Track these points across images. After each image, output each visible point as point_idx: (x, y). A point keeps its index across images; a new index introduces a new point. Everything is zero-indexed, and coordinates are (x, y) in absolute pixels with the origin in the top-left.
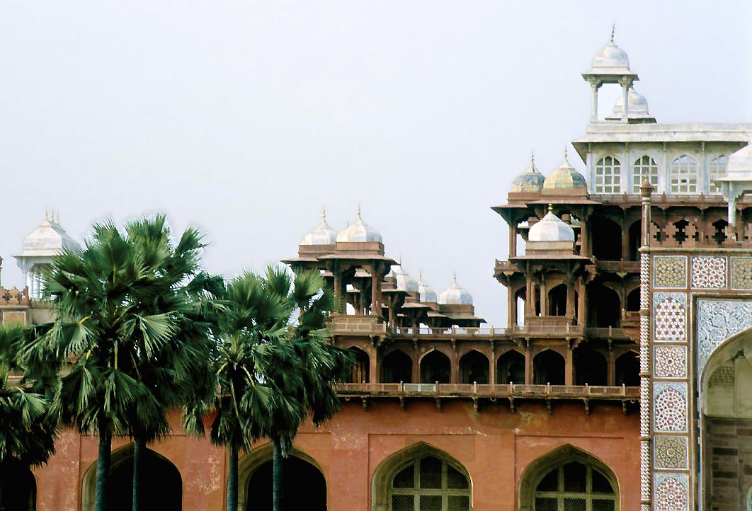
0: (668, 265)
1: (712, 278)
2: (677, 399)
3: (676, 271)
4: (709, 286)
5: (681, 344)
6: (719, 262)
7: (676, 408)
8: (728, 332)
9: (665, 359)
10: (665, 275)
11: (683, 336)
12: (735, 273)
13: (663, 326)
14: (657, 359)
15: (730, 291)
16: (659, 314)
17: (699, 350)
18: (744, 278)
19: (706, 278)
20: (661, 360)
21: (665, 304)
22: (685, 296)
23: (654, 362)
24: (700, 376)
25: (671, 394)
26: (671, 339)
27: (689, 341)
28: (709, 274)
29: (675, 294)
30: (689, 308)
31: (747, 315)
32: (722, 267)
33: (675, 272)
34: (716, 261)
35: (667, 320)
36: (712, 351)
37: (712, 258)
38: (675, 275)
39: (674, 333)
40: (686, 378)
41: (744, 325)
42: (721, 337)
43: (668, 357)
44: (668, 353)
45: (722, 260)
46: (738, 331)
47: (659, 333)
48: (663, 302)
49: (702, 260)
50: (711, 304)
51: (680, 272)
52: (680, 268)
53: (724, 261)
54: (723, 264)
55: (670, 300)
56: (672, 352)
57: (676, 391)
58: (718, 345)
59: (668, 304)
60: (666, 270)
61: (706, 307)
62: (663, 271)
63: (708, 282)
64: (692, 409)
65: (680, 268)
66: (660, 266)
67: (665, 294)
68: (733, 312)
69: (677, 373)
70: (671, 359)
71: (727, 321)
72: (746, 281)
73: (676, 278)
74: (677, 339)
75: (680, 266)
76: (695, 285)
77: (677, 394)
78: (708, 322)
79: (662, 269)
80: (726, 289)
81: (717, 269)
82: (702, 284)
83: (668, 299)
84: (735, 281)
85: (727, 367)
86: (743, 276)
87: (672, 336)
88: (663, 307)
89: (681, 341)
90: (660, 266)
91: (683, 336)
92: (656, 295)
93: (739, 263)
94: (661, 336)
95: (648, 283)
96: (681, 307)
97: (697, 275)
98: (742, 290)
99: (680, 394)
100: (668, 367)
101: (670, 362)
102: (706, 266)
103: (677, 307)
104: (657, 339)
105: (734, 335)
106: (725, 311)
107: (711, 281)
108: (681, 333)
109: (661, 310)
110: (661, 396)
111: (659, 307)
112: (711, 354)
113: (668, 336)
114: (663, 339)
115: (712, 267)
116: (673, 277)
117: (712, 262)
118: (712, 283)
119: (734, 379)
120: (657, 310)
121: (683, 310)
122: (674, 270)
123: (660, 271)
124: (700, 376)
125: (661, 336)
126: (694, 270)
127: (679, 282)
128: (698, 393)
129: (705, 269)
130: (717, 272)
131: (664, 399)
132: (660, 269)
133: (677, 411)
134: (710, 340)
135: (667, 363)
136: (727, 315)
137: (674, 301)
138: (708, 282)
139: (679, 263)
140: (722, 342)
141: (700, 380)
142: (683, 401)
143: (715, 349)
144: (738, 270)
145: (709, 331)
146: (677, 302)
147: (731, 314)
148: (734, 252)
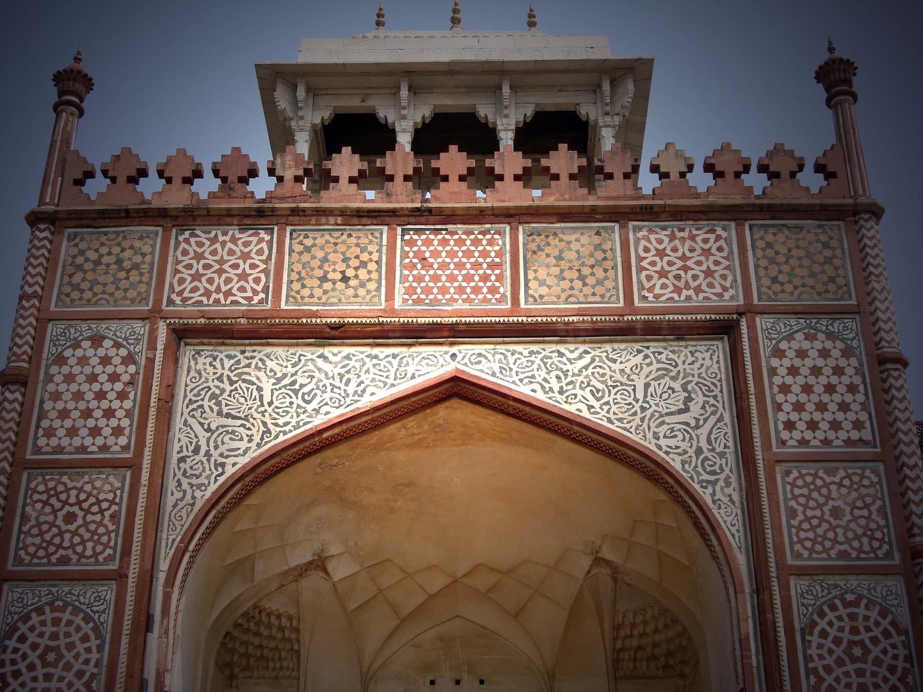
0: (104, 250)
1: (228, 281)
2: (76, 638)
3: (127, 264)
4: (217, 301)
5: (115, 465)
6: (254, 239)
7: (68, 667)
8: (269, 431)
9: (54, 512)
10: (90, 276)
11: (123, 441)
12: (297, 267)
13: (64, 414)
14: (29, 509)
15: (276, 312)
16: (58, 379)
17: (171, 485)
18: (324, 279)
19: (211, 281)
20: (41, 512)
21: (79, 353)
22: (140, 328)
23: (17, 520)
24: (164, 566)
25: (56, 622)
26: (83, 449)
27: (139, 453)
28: (220, 272)
29: (114, 325)
30: (151, 361)
31: (327, 382)
32: (260, 252)
33: (121, 269)
34: (244, 237)
35: (78, 396)
36: (213, 488)
37: (233, 231)
38: (122, 274)
39: (95, 432)
40: (114, 566)
41: (317, 411)
42: (243, 445)
43: (65, 503)
44: (67, 490)
45: (263, 234)
46: (295, 428)
47: (50, 433)
48: (76, 345)
49: (203, 237)
50: (221, 356)
51: (136, 267)
52: (138, 259)
53: (267, 238)
54: (264, 245)
55: (97, 341)
56: (81, 490)
57: (76, 611)
58: (230, 471)
59: (90, 353)
60: (97, 263)
61: (203, 367)
62: (88, 266)
63: (218, 290)
64: (122, 668)
65: (138, 259)
66: (82, 253)
67: (84, 326)
68: (285, 376)
69: (89, 552)
70: (76, 509)
71: (267, 399)
72: (328, 286)
73: (124, 284)
74: (104, 448)
75: (137, 251)
76: (178, 300)
77: (78, 620)
78: (206, 403)
79: (87, 260)
80: (269, 306)
81: (245, 256)
82: (196, 297)
83: (90, 338)
84: (296, 286)
85: (279, 617)
86: (320, 273)
87: (88, 441)
88: (72, 361)
89: (116, 452)
90: (82, 253)
91: (123, 441)
92: (52, 330)
93: (308, 242)
94: (54, 442)
95: (40, 299)
96: (129, 360)
97: (186, 274)
98: (315, 308)
99: (87, 619)
100: (61, 534)
101: (70, 518)
102: (214, 253)
103: (117, 360)
104: (37, 450)
105: (282, 438)
106: (261, 374)
107: (224, 288)
108: (118, 431)
109: (65, 370)
110: (23, 628)
111: (61, 360)
112: (208, 494)
113: (77, 442)
114: (60, 450)
115: (231, 252)
116: (116, 282)
117: (234, 240)
118: (228, 293)
119: (298, 653)
120: (54, 369)
121: (132, 369)
122: (119, 262)
123: (80, 267)
124: (164, 566)
125: (54, 442)
126: (178, 262)
127: (132, 294)
128: (149, 618)
129: (210, 260)
130: (245, 266)
131: (32, 638)
132: (80, 260)
133: (70, 676)
134: (208, 454)
135: (59, 522)
136: (267, 386)
137: (107, 343)
138: (218, 290)
139: (137, 244)
140: (243, 461)
141: (162, 577)
142: (94, 643)
143: (221, 480)
144: (306, 257)
145: (208, 430)
146: (117, 345)
147: (279, 380)
148: (295, 212)
